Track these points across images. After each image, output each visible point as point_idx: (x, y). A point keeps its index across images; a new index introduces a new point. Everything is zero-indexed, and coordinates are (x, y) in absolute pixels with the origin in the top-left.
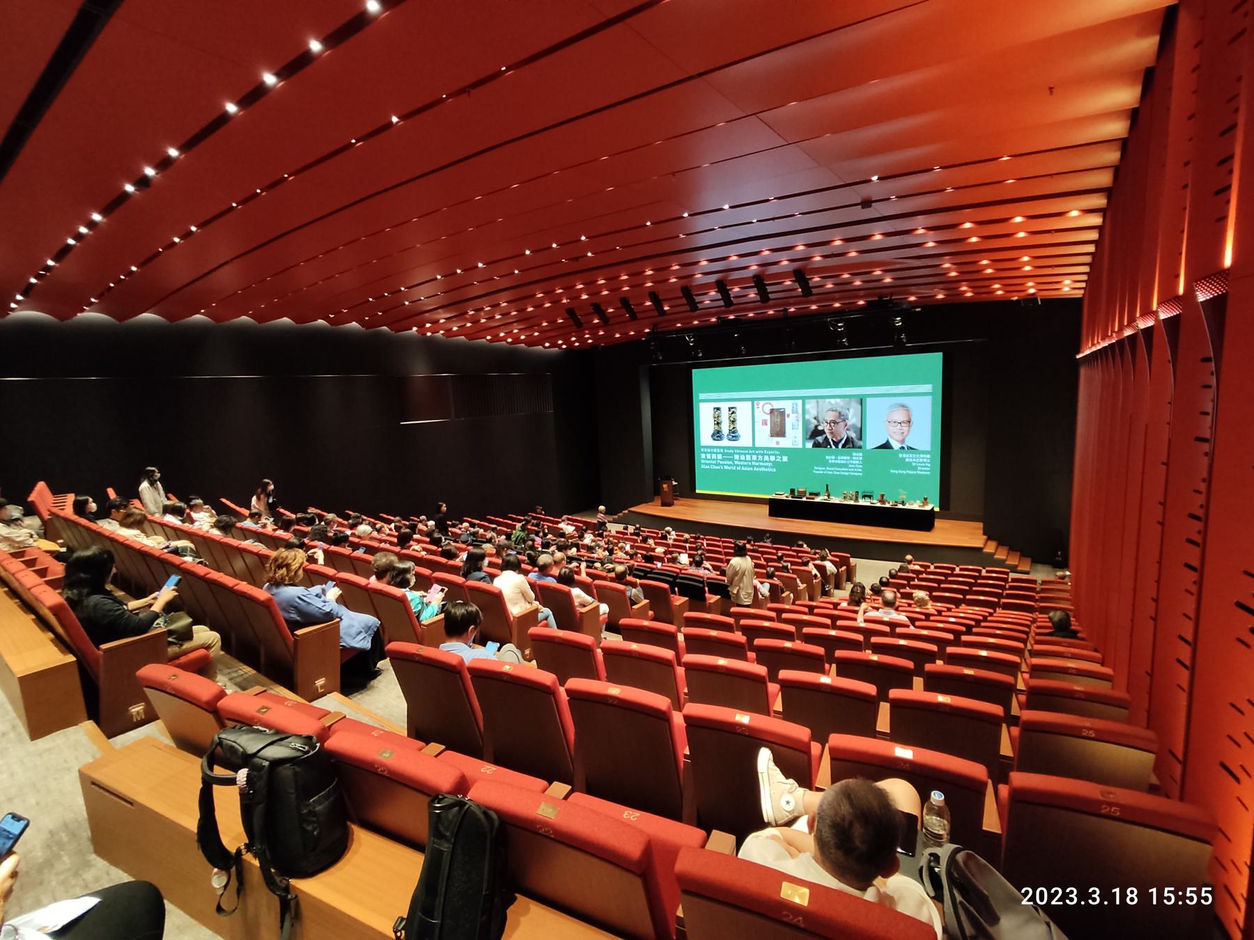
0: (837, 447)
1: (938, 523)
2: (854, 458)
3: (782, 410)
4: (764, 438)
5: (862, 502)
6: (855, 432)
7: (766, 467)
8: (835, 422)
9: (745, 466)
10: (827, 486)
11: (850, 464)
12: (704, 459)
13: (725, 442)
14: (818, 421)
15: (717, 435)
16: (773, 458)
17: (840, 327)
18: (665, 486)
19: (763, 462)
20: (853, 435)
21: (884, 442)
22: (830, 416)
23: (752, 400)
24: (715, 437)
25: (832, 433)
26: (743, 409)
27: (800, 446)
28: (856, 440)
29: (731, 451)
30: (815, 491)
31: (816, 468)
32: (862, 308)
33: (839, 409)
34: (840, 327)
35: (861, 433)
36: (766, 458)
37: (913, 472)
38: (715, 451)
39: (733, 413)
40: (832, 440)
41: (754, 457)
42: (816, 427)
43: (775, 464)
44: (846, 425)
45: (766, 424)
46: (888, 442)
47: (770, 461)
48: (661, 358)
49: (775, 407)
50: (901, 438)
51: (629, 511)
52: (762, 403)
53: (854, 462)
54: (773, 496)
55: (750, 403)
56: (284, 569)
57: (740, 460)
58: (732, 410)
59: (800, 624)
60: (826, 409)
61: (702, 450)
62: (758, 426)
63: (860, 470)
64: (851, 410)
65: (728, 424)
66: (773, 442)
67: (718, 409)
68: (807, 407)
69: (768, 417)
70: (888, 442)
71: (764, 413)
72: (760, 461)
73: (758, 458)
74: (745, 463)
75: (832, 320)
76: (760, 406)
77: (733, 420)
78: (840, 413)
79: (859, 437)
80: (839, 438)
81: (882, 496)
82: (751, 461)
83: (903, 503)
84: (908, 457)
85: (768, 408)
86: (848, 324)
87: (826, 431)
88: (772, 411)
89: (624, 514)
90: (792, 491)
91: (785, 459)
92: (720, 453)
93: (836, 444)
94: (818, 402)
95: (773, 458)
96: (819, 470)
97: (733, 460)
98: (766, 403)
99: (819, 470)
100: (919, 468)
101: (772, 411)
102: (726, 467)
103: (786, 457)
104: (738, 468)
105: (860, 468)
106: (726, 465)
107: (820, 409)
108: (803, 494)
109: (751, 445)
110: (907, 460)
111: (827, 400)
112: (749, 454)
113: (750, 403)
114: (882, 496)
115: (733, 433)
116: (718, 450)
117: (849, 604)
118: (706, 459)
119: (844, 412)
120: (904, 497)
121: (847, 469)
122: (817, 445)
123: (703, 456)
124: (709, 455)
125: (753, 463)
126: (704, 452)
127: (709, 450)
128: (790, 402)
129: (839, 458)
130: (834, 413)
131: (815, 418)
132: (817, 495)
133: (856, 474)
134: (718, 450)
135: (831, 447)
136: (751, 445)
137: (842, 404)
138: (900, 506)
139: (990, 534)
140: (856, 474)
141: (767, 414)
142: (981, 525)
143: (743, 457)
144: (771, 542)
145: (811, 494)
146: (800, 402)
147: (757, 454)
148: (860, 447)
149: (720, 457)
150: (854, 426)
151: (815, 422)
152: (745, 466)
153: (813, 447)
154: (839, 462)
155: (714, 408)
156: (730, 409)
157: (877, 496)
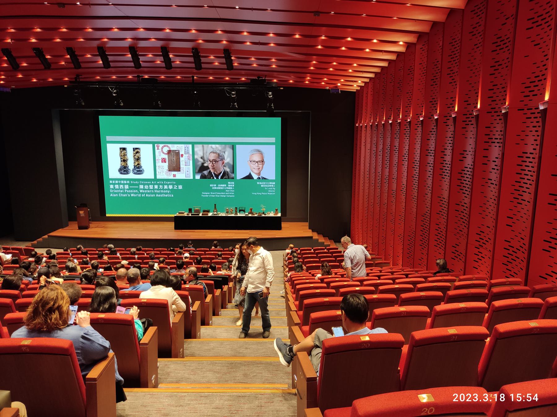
0: (217, 178)
1: (284, 225)
2: (229, 186)
3: (177, 151)
4: (164, 173)
5: (239, 215)
6: (229, 168)
7: (166, 194)
8: (216, 161)
9: (148, 193)
10: (215, 205)
11: (227, 189)
12: (113, 189)
13: (131, 176)
14: (204, 160)
15: (124, 170)
16: (171, 187)
17: (233, 95)
18: (81, 212)
19: (163, 189)
20: (228, 169)
21: (248, 174)
22: (212, 157)
23: (154, 143)
24: (122, 171)
25: (213, 168)
26: (146, 151)
27: (192, 178)
28: (230, 173)
30: (206, 209)
31: (203, 193)
32: (244, 84)
33: (218, 152)
34: (233, 95)
35: (233, 168)
36: (166, 187)
37: (265, 194)
38: (122, 182)
39: (137, 152)
40: (214, 173)
41: (156, 187)
42: (203, 164)
43: (172, 191)
44: (223, 163)
45: (165, 162)
46: (250, 174)
47: (169, 189)
48: (122, 104)
49: (172, 149)
50: (257, 171)
51: (48, 236)
52: (161, 146)
53: (229, 188)
54: (177, 214)
55: (151, 145)
56: (57, 312)
58: (136, 150)
59: (376, 285)
60: (209, 152)
61: (111, 182)
62: (159, 164)
64: (226, 153)
65: (133, 161)
66: (170, 176)
67: (124, 149)
68: (196, 149)
69: (166, 157)
70: (250, 174)
71: (163, 153)
72: (161, 190)
73: (158, 187)
75: (228, 89)
76: (160, 148)
77: (137, 158)
78: (219, 155)
79: (232, 172)
80: (219, 172)
81: (251, 210)
83: (264, 213)
84: (263, 184)
85: (166, 150)
86: (238, 92)
87: (210, 167)
88: (169, 152)
89: (43, 239)
90: (190, 210)
91: (180, 187)
92: (127, 184)
93: (217, 176)
94: (203, 146)
95: (171, 187)
96: (205, 194)
97: (138, 189)
98: (165, 146)
99: (205, 194)
100: (270, 191)
101: (169, 152)
102: (132, 195)
103: (275, 183)
104: (143, 195)
105: (233, 192)
106: (132, 193)
107: (205, 152)
108: (198, 211)
109: (153, 178)
110: (262, 186)
111: (210, 145)
112: (151, 184)
113: (151, 145)
114: (251, 210)
115: (138, 168)
116: (125, 182)
117: (322, 275)
118: (114, 188)
119: (221, 154)
120: (265, 209)
121: (225, 193)
122: (203, 177)
123: (112, 186)
124: (117, 186)
126: (112, 184)
127: (117, 182)
128: (183, 145)
129: (219, 185)
130: (215, 154)
131: (201, 158)
132: (208, 211)
133: (231, 196)
134: (125, 182)
135: (213, 178)
136: (153, 178)
138: (263, 215)
139: (312, 228)
140: (231, 196)
141: (165, 154)
142: (307, 224)
143: (146, 187)
144: (193, 247)
145: (204, 211)
146: (190, 146)
147: (159, 185)
148: (233, 178)
149: (127, 187)
150: (228, 163)
151: (202, 161)
152: (148, 193)
153: (201, 178)
154: (219, 188)
155: (120, 148)
156: (134, 149)
157: (248, 210)
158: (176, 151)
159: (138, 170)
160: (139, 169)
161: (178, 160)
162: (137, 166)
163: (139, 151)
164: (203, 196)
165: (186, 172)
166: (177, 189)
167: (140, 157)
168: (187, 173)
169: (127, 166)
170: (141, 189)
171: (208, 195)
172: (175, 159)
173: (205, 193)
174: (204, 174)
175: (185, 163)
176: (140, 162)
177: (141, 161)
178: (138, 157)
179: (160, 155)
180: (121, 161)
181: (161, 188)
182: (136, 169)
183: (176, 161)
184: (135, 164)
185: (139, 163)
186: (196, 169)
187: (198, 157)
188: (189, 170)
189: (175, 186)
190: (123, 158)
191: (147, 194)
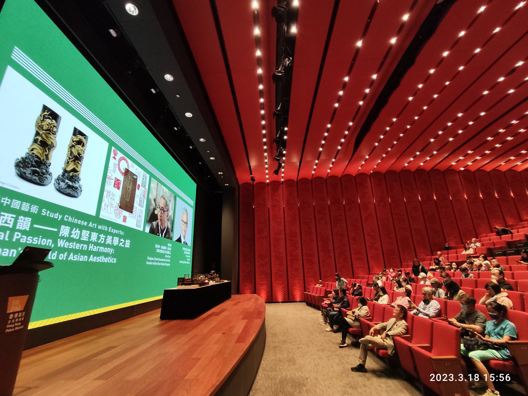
3: (135, 177)
7: (106, 255)
9: (76, 252)
29: (57, 216)
31: (149, 258)
39: (80, 142)
40: (160, 227)
41: (94, 236)
49: (131, 169)
57: (70, 239)
58: (80, 137)
62: (110, 187)
63: (169, 261)
67: (55, 116)
69: (121, 178)
73: (99, 238)
74: (78, 246)
77: (76, 154)
82: (88, 243)
85: (124, 165)
88: (127, 173)
98: (124, 159)
109: (94, 214)
115: (71, 179)
122: (153, 231)
125: (91, 247)
137: (168, 194)
152: (76, 252)
158: (134, 175)
160: (72, 181)
162: (71, 174)
163: (84, 140)
164: (151, 263)
167: (82, 155)
169: (48, 162)
170: (63, 238)
176: (79, 166)
177: (81, 165)
178: (79, 154)
180: (35, 141)
181: (102, 240)
182: (67, 181)
184: (67, 166)
185: (77, 169)
186: (147, 217)
187: (152, 197)
188: (141, 214)
190: (43, 135)
191: (72, 254)
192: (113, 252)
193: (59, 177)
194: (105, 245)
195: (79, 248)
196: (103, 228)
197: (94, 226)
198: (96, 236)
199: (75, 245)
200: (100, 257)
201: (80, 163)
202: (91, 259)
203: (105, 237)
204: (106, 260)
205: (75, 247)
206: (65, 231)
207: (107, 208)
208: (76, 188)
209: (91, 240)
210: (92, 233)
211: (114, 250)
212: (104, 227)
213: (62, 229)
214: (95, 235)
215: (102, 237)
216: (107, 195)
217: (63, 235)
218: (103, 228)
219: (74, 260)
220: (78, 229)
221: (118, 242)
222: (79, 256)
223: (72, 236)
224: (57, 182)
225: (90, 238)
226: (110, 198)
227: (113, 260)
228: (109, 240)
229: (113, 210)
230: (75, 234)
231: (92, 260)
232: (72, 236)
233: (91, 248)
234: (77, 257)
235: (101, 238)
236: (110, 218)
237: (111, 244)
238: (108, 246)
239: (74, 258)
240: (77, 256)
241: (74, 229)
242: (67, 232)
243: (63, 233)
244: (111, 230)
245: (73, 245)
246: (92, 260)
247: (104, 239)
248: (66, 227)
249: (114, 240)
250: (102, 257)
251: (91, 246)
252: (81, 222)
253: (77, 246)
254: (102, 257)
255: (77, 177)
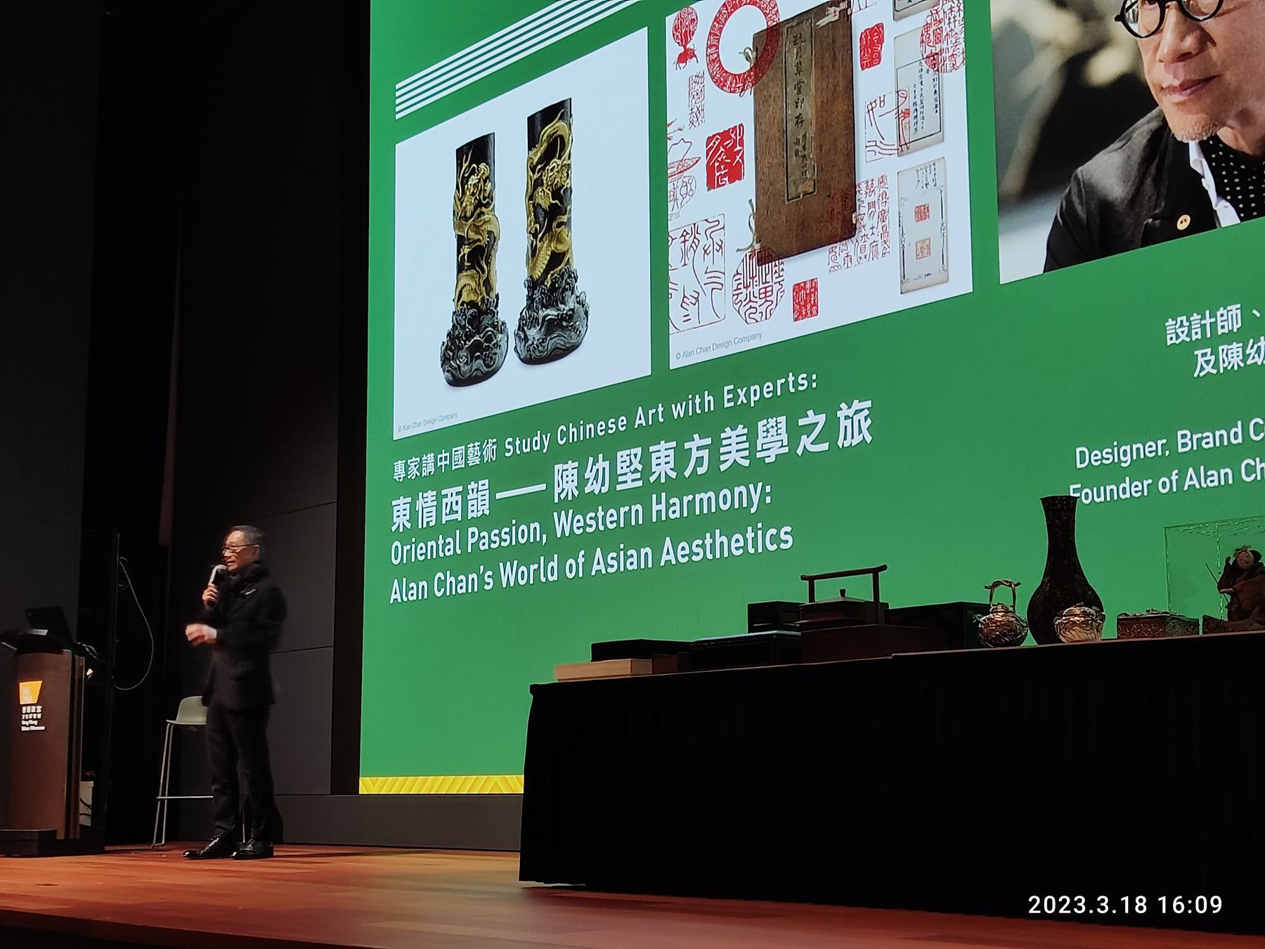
7: (733, 521)
9: (608, 540)
41: (663, 456)
57: (584, 502)
73: (682, 457)
74: (612, 518)
152: (608, 540)
159: (552, 313)
161: (840, 106)
165: (909, 215)
166: (825, 446)
168: (918, 231)
170: (564, 505)
171: (1141, 468)
172: (808, 109)
173: (1106, 456)
174: (1089, 191)
175: (902, 115)
179: (697, 114)
181: (700, 461)
183: (823, 127)
185: (561, 248)
186: (1002, 165)
188: (931, 198)
189: (811, 417)
190: (473, 235)
192: (768, 500)
193: (522, 319)
194: (716, 479)
195: (618, 522)
196: (694, 404)
197: (655, 415)
198: (671, 452)
199: (604, 517)
200: (704, 539)
201: (564, 219)
202: (668, 553)
203: (708, 441)
204: (734, 545)
205: (604, 523)
206: (566, 479)
207: (692, 310)
208: (570, 316)
209: (652, 479)
210: (652, 449)
211: (768, 489)
212: (698, 400)
213: (557, 477)
214: (667, 453)
215: (698, 449)
216: (685, 253)
217: (562, 496)
218: (694, 404)
219: (610, 570)
220: (601, 456)
221: (784, 437)
222: (622, 553)
223: (587, 490)
224: (520, 337)
225: (646, 471)
226: (700, 251)
227: (776, 539)
228: (733, 448)
229: (724, 299)
230: (596, 478)
231: (671, 557)
232: (587, 490)
233: (659, 512)
234: (617, 559)
235: (695, 454)
236: (428, 422)
237: (746, 463)
238: (737, 475)
239: (607, 565)
240: (614, 555)
241: (591, 459)
242: (405, 515)
243: (563, 490)
244: (737, 396)
245: (596, 518)
246: (671, 557)
247: (705, 453)
248: (565, 467)
249: (761, 434)
250: (713, 537)
251: (659, 503)
252: (607, 425)
253: (608, 519)
254: (713, 537)
255: (566, 276)
